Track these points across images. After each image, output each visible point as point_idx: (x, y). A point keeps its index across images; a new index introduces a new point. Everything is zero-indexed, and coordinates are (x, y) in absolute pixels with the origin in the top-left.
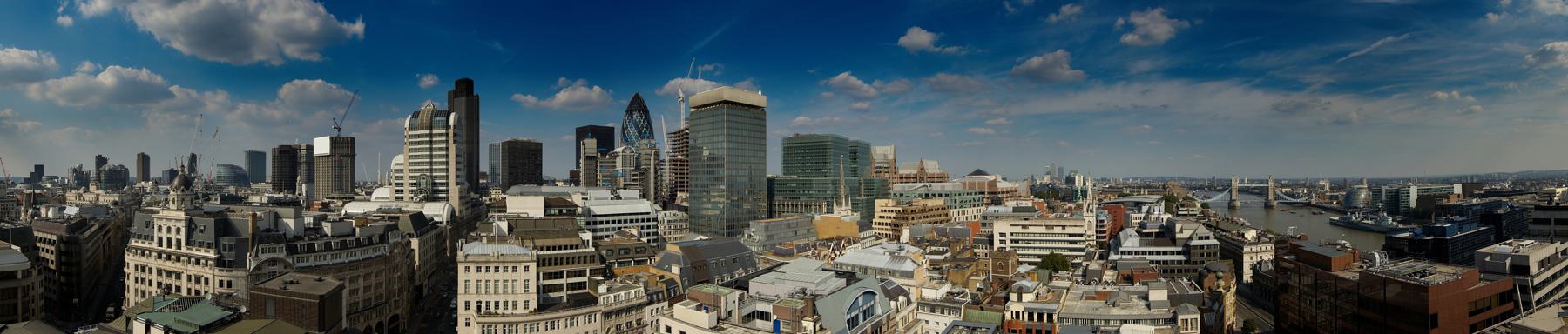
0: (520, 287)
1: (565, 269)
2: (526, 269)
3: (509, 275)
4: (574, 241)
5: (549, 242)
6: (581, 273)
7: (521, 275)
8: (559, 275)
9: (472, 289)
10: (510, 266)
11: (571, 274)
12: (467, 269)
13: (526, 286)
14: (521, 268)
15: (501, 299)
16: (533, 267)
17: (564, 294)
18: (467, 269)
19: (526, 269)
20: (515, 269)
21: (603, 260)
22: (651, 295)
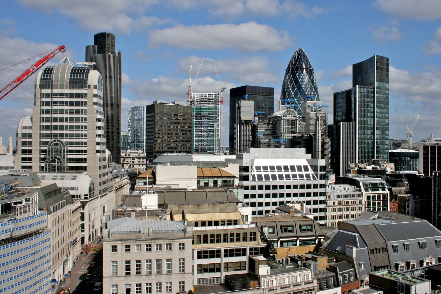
0: (176, 268)
1: (222, 246)
2: (182, 246)
3: (164, 254)
4: (233, 216)
5: (204, 217)
6: (242, 252)
7: (176, 254)
8: (215, 254)
9: (122, 270)
10: (164, 243)
11: (229, 253)
12: (114, 249)
13: (182, 265)
14: (176, 245)
15: (153, 280)
16: (188, 243)
17: (222, 275)
18: (114, 249)
19: (182, 246)
20: (169, 247)
21: (264, 239)
22: (320, 280)
